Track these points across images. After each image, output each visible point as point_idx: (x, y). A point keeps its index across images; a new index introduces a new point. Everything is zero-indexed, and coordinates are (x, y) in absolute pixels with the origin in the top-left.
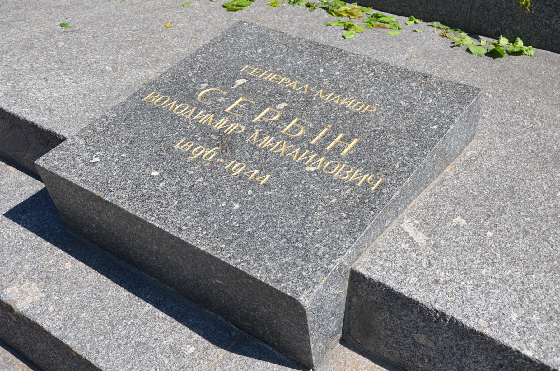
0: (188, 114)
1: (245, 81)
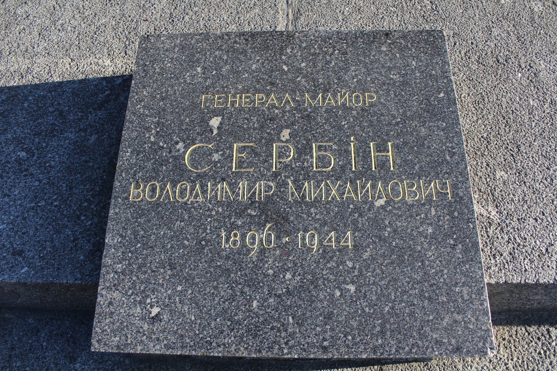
0: (197, 196)
1: (219, 119)
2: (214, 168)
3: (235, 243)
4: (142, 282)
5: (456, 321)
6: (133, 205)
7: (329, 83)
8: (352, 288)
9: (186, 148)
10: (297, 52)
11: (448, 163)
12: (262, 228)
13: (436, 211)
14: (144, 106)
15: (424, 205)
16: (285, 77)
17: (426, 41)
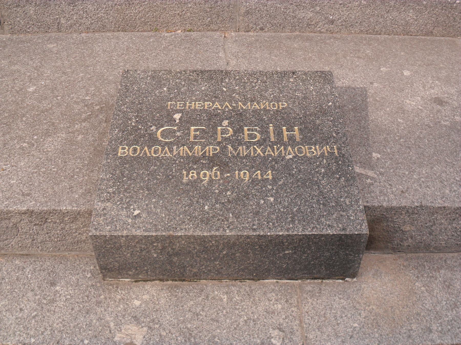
1: (180, 114)
2: (177, 140)
3: (192, 177)
4: (127, 197)
5: (342, 216)
6: (121, 158)
7: (254, 97)
8: (272, 199)
9: (157, 129)
10: (233, 81)
11: (334, 137)
12: (211, 170)
13: (327, 161)
14: (127, 108)
16: (224, 94)
17: (320, 77)
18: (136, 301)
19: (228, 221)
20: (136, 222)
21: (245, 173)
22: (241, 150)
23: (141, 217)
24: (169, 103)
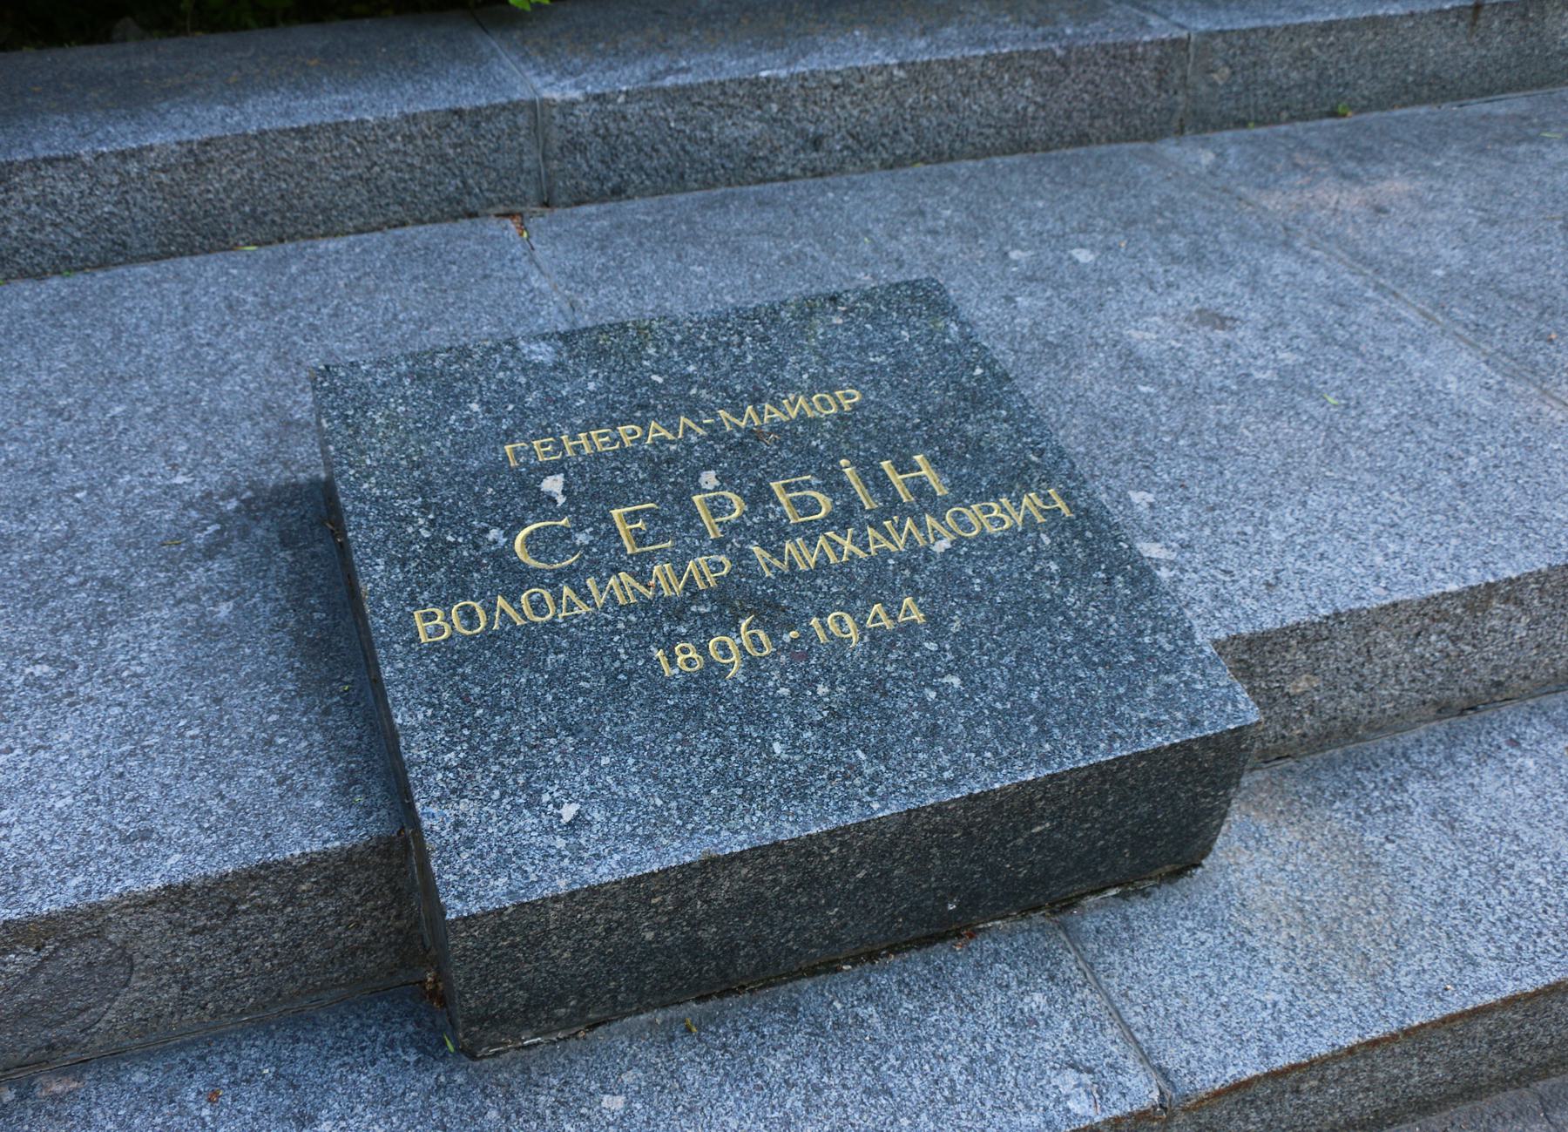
0: (571, 606)
3: (689, 662)
4: (516, 771)
5: (1168, 686)
6: (434, 648)
7: (756, 389)
9: (510, 535)
11: (1038, 466)
15: (1024, 533)
18: (606, 1097)
19: (861, 774)
20: (583, 841)
21: (840, 620)
22: (795, 553)
23: (589, 824)
24: (508, 448)
